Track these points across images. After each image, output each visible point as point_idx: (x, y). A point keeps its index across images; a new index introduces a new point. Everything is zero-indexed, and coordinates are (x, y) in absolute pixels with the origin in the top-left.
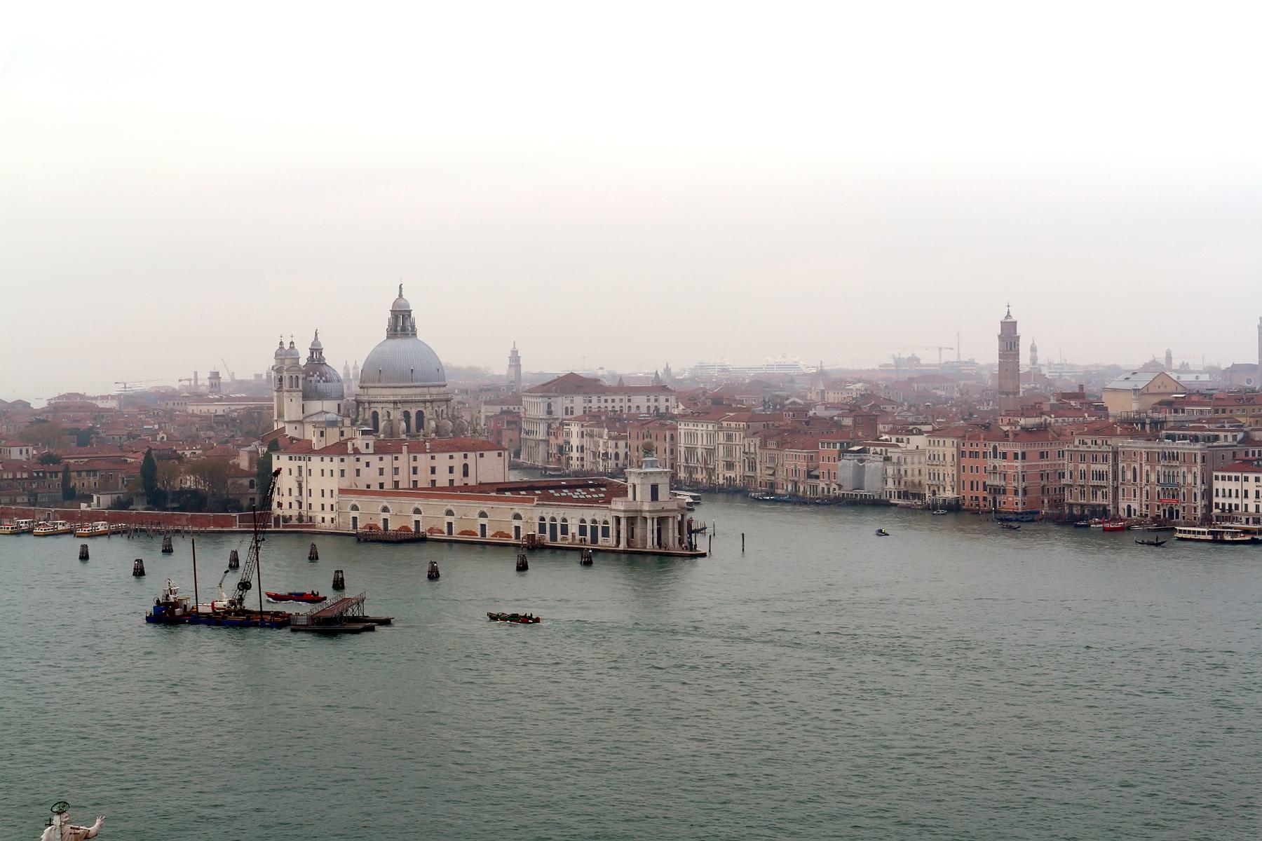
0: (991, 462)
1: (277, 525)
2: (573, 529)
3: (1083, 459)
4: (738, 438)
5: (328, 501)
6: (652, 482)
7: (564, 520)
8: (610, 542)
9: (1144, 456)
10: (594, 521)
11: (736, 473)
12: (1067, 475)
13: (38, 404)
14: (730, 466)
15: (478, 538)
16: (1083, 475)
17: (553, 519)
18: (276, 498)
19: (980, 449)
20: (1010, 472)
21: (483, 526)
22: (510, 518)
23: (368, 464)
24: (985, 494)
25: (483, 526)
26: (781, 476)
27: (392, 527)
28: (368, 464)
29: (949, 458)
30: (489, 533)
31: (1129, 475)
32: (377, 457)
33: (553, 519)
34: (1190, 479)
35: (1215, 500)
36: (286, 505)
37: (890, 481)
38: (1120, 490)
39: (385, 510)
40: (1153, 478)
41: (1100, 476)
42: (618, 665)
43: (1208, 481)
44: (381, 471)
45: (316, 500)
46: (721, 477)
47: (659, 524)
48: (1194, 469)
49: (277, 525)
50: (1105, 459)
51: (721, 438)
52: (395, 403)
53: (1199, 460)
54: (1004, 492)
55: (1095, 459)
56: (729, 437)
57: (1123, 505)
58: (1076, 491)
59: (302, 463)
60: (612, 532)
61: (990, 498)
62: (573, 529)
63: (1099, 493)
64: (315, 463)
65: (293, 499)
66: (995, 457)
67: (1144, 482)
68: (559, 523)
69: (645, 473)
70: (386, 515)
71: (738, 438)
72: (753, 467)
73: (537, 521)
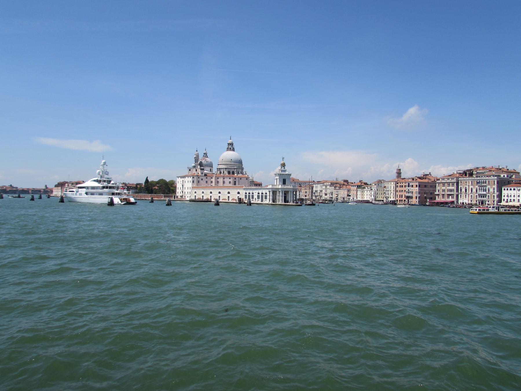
0: (407, 188)
1: (175, 198)
2: (256, 197)
3: (444, 185)
4: (328, 187)
5: (189, 191)
6: (284, 178)
7: (253, 193)
8: (267, 201)
9: (470, 183)
10: (262, 193)
11: (328, 197)
12: (437, 191)
13: (168, 180)
14: (326, 194)
15: (227, 201)
16: (444, 191)
17: (249, 193)
18: (177, 191)
19: (404, 184)
20: (414, 191)
21: (229, 197)
22: (236, 193)
23: (202, 179)
24: (405, 199)
25: (229, 197)
26: (339, 196)
27: (205, 198)
28: (202, 179)
29: (392, 188)
30: (230, 199)
31: (463, 190)
32: (205, 177)
33: (249, 193)
34: (491, 190)
35: (503, 198)
36: (179, 193)
37: (372, 196)
38: (459, 195)
39: (203, 193)
40: (474, 190)
41: (451, 190)
42: (42, 253)
43: (500, 191)
44: (207, 182)
45: (186, 191)
46: (324, 197)
47: (285, 194)
48: (493, 186)
49: (175, 198)
50: (453, 185)
51: (324, 187)
52: (226, 168)
53: (496, 183)
54: (412, 198)
55: (449, 185)
56: (326, 187)
57: (460, 201)
58: (441, 196)
59: (183, 179)
60: (268, 197)
61: (407, 200)
62: (256, 197)
63: (450, 197)
64: (187, 179)
65: (181, 191)
66: (409, 186)
67: (470, 192)
68: (251, 194)
69: (281, 174)
70: (203, 195)
71: (328, 187)
72: (332, 194)
73: (244, 194)
